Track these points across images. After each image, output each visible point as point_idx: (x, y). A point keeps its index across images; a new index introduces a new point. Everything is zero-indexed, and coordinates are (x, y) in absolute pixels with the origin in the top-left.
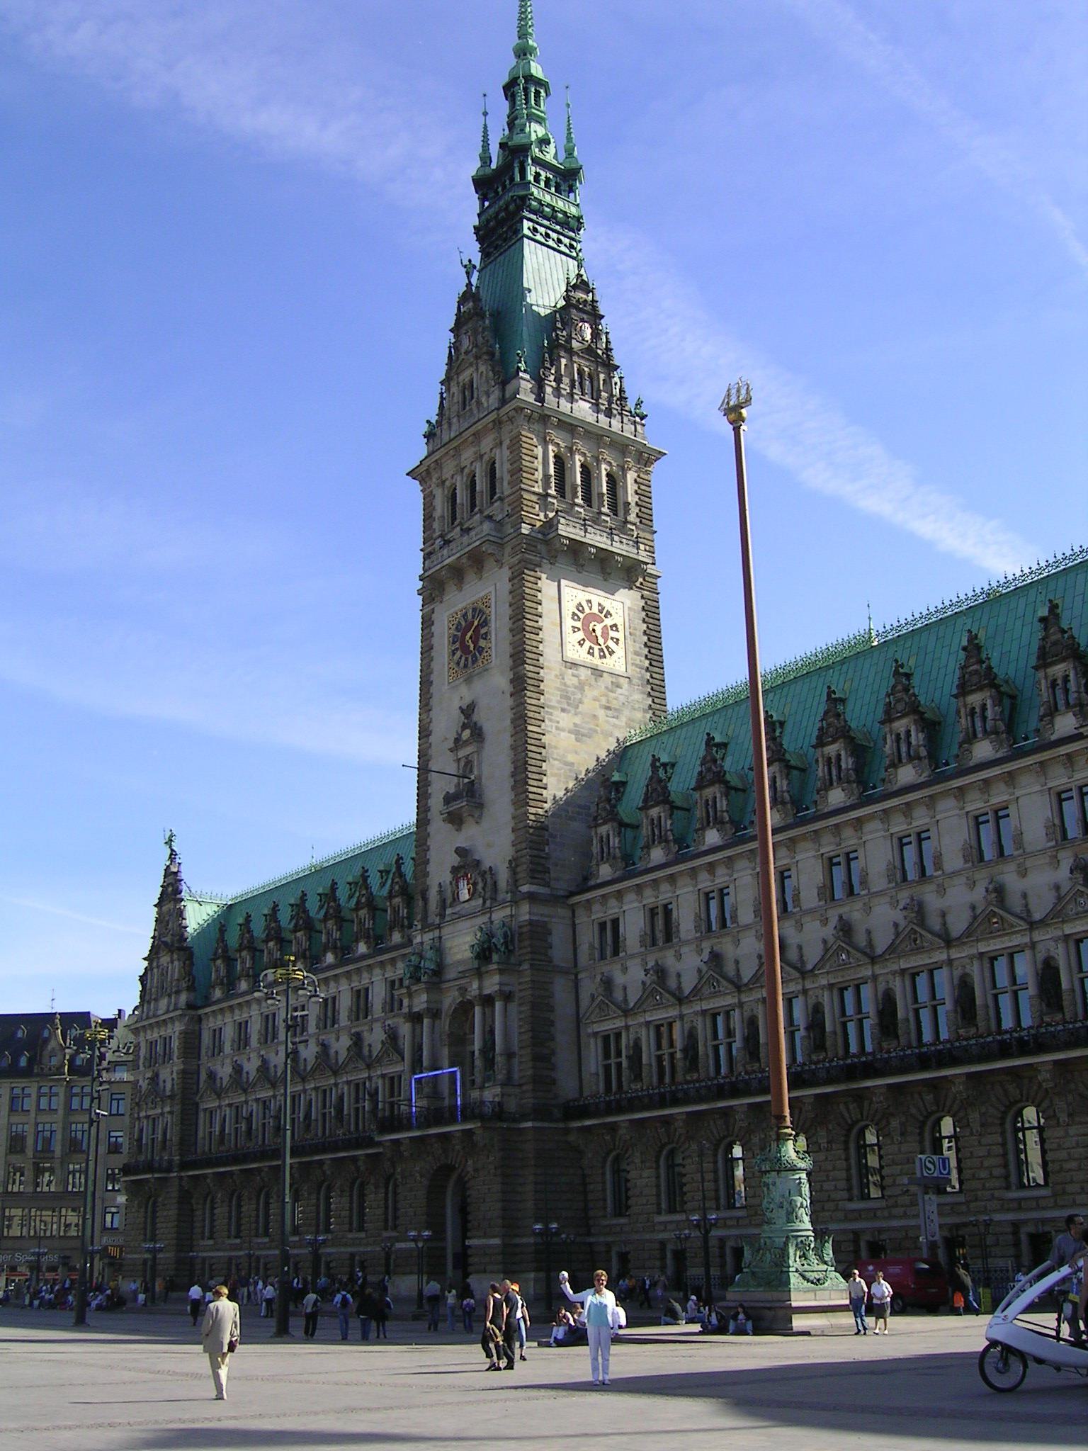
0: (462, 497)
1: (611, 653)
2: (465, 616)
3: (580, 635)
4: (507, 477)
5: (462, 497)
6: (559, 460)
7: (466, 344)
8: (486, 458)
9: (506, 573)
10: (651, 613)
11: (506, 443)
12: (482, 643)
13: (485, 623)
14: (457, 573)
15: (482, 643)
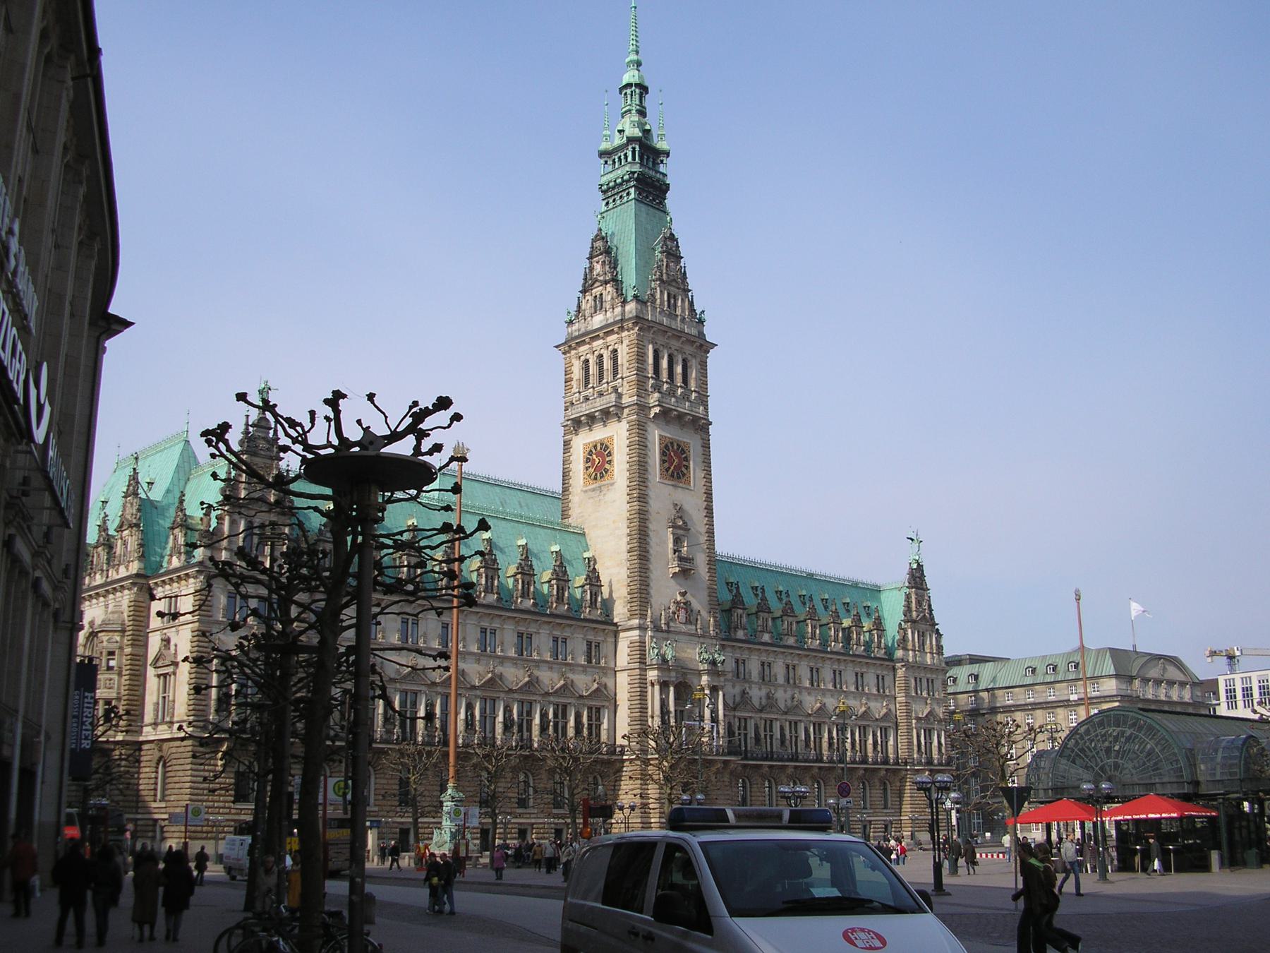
0: (593, 369)
1: (684, 475)
2: (595, 446)
3: (666, 465)
4: (626, 365)
5: (593, 369)
6: (656, 353)
7: (598, 268)
8: (611, 348)
9: (624, 425)
10: (706, 446)
11: (626, 342)
12: (607, 466)
13: (610, 454)
14: (591, 419)
15: (607, 466)
